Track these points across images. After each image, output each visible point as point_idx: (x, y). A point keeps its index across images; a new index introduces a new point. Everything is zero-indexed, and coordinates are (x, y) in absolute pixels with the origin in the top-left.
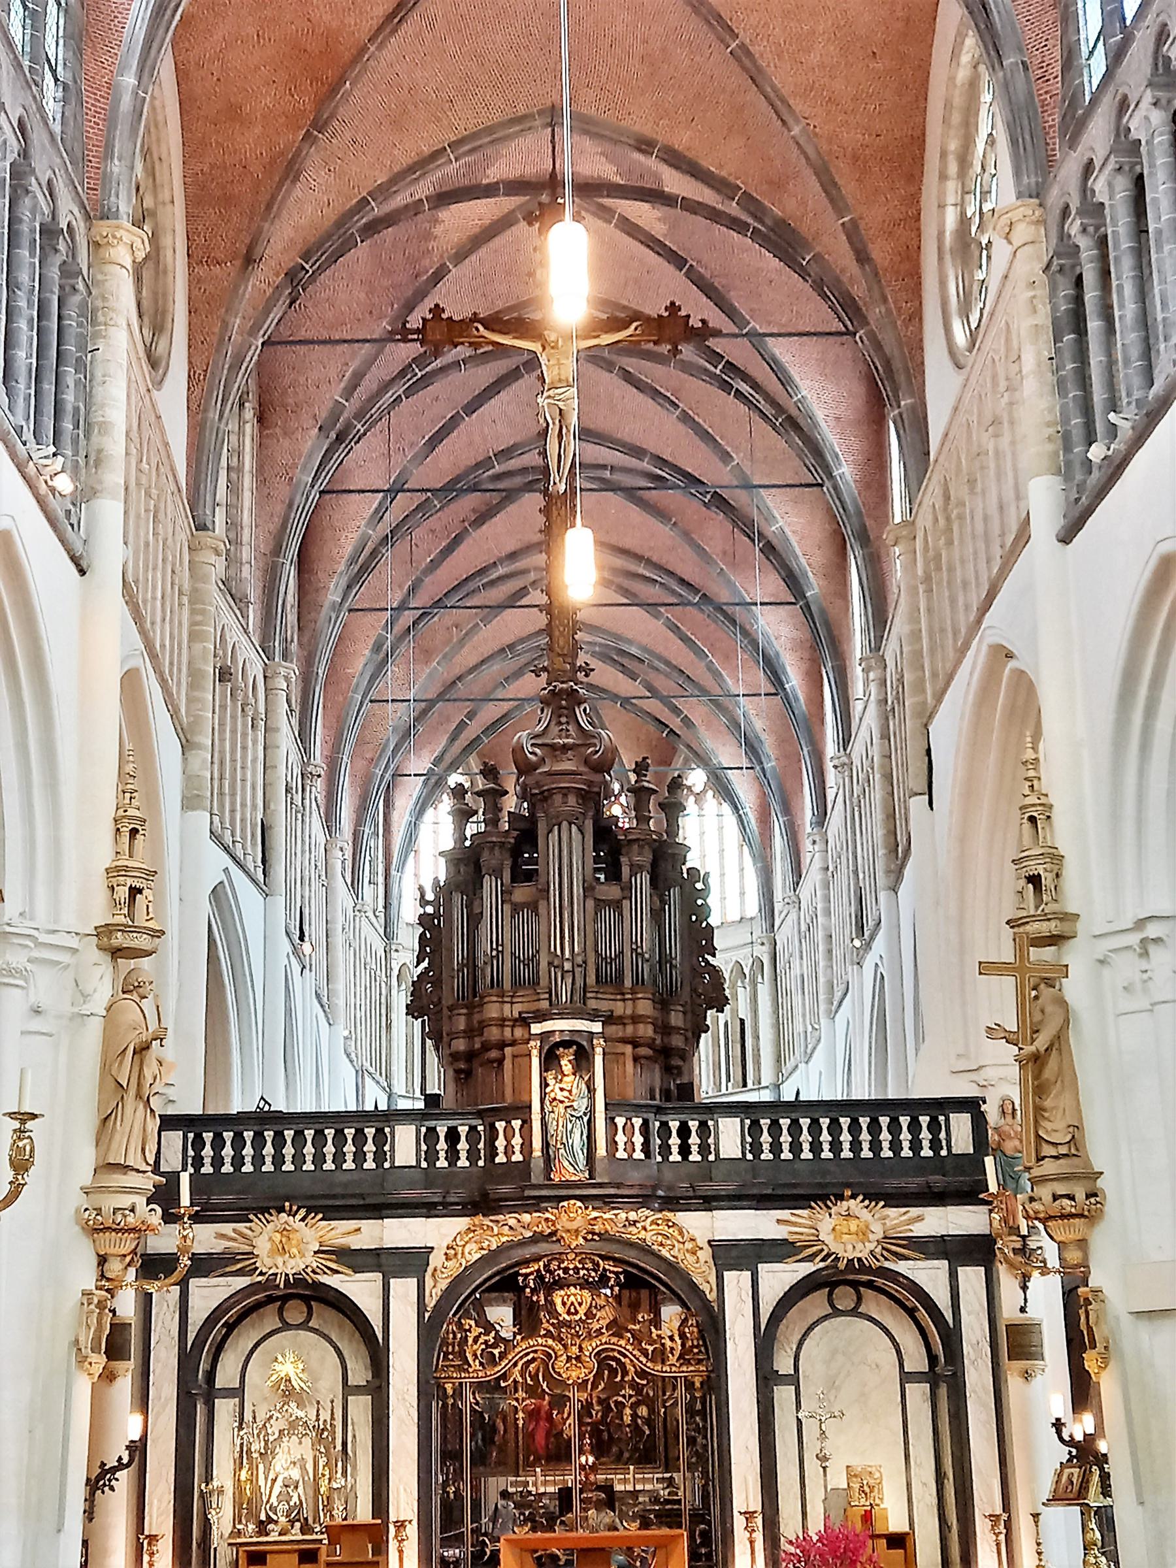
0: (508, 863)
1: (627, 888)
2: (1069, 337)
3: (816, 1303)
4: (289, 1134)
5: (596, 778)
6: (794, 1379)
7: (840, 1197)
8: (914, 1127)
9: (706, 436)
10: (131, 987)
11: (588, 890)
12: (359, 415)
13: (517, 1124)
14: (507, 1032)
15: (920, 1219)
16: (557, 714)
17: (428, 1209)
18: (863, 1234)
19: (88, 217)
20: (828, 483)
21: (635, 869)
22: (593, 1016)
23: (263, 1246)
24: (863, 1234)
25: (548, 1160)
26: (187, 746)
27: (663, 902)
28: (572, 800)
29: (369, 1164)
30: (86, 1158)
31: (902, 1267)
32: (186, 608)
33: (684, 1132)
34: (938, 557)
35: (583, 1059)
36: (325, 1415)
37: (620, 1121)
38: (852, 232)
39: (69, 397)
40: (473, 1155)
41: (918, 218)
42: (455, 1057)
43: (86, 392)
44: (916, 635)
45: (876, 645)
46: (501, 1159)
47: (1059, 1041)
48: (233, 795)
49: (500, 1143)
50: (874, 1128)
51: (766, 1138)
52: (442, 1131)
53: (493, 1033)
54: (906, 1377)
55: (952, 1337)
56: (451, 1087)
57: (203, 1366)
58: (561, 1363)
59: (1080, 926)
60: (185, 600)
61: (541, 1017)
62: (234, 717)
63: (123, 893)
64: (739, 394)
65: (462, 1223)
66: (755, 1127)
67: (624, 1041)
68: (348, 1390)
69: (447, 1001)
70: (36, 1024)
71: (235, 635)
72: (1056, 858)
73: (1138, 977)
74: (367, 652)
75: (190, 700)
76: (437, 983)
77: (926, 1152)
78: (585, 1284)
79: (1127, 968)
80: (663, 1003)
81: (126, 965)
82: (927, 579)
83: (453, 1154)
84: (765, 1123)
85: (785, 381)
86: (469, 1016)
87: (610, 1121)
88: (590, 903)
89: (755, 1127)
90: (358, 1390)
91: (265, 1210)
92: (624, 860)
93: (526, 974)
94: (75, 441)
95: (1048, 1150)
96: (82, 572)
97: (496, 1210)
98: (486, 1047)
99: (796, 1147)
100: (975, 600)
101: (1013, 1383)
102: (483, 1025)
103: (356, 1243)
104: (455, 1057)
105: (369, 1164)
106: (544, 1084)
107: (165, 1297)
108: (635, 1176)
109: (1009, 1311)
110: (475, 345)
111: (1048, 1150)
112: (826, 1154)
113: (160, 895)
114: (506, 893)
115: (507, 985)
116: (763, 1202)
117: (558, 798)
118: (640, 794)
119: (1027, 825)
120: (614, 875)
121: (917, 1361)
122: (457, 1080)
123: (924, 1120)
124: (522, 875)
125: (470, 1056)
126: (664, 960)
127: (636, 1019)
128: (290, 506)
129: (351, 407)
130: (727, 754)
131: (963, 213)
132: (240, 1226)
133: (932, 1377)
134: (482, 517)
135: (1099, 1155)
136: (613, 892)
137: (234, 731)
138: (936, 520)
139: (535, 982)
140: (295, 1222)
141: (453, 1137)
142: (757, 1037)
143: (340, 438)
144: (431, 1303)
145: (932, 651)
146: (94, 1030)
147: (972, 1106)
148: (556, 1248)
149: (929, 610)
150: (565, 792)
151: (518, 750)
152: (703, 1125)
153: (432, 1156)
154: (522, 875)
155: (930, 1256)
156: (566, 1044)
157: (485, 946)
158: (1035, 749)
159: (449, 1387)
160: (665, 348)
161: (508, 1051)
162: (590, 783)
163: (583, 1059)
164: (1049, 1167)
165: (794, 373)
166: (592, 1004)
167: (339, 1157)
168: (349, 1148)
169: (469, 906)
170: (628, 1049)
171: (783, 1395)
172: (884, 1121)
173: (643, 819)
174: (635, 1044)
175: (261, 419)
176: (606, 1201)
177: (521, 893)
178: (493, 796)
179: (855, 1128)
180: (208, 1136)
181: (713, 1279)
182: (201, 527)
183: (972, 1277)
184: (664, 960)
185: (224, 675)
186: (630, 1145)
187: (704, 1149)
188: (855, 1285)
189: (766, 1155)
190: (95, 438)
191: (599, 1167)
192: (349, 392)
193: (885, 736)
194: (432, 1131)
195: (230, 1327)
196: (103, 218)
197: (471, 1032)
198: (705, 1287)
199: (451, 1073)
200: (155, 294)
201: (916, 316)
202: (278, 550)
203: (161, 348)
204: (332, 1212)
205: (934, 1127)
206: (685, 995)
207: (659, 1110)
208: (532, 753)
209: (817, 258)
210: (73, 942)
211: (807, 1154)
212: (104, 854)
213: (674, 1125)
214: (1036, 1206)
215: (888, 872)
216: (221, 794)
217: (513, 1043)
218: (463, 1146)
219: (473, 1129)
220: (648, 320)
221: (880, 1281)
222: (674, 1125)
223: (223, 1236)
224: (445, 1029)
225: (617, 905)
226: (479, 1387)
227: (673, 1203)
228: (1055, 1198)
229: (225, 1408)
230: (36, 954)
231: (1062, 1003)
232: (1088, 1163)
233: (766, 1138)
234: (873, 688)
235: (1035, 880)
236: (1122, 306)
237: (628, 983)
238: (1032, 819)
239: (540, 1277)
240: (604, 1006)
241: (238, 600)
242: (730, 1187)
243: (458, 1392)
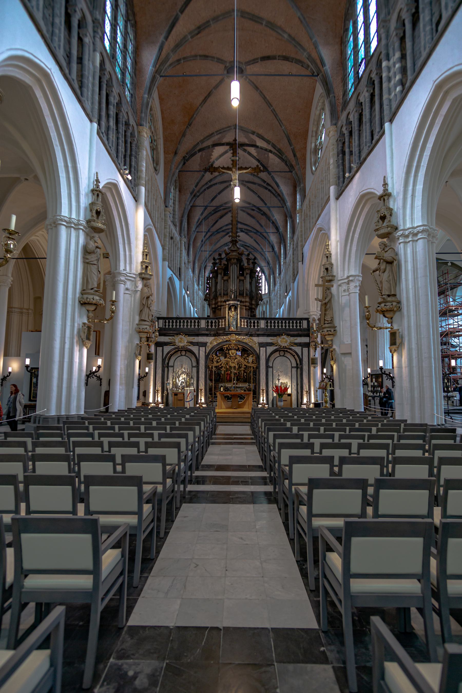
0: (223, 272)
1: (245, 278)
2: (341, 155)
3: (277, 354)
4: (182, 321)
5: (240, 256)
6: (272, 367)
7: (282, 335)
8: (296, 323)
9: (262, 200)
10: (145, 285)
11: (238, 277)
12: (198, 191)
13: (223, 320)
14: (222, 304)
15: (297, 339)
16: (233, 245)
17: (207, 335)
18: (286, 342)
19: (137, 125)
20: (285, 207)
21: (247, 274)
22: (238, 301)
23: (177, 341)
24: (286, 342)
25: (229, 327)
26: (163, 249)
27: (252, 281)
28: (235, 260)
29: (196, 327)
30: (137, 318)
31: (293, 348)
32: (163, 223)
33: (254, 323)
34: (307, 214)
35: (236, 309)
36: (189, 371)
37: (243, 320)
38: (293, 151)
39: (133, 164)
40: (215, 326)
41: (306, 148)
42: (212, 308)
43: (137, 163)
44: (301, 231)
45: (292, 238)
46: (220, 326)
47: (330, 300)
48: (173, 261)
49: (220, 324)
50: (289, 323)
51: (269, 324)
52: (210, 321)
53: (219, 304)
54: (292, 367)
55: (301, 360)
56: (212, 314)
57: (166, 362)
58: (230, 363)
59: (336, 278)
60: (163, 221)
61: (228, 301)
62: (174, 247)
63: (144, 266)
64: (269, 190)
65: (213, 338)
66: (267, 322)
67: (244, 306)
68: (192, 367)
69: (211, 298)
70: (127, 292)
71: (174, 231)
72: (332, 264)
73: (346, 288)
74: (200, 242)
75: (164, 240)
76: (209, 295)
77: (298, 327)
78: (235, 349)
79: (345, 287)
80: (251, 298)
81: (145, 281)
82: (304, 220)
83: (212, 326)
84: (269, 321)
85: (278, 186)
86: (215, 301)
87: (241, 320)
88: (238, 280)
89: (267, 322)
90: (194, 367)
91: (177, 334)
92: (245, 272)
93: (225, 293)
94: (135, 173)
95: (326, 322)
96: (136, 201)
97: (220, 336)
98: (218, 306)
99: (275, 326)
100: (314, 220)
101: (312, 368)
102: (218, 302)
103: (194, 341)
104: (212, 308)
105: (196, 327)
106: (229, 313)
107: (159, 349)
108: (245, 330)
109: (312, 356)
110: (219, 172)
111: (326, 322)
112: (280, 327)
113: (152, 267)
114: (222, 278)
115: (222, 295)
116: (268, 335)
117: (232, 260)
118: (248, 260)
119: (326, 258)
120: (242, 275)
121: (294, 364)
122: (213, 313)
123: (298, 322)
124: (225, 275)
125: (215, 308)
126: (251, 291)
127: (246, 302)
128: (185, 208)
129: (197, 189)
130: (263, 264)
131: (316, 144)
132: (173, 337)
133: (297, 368)
134: (221, 217)
135: (336, 323)
136: (242, 278)
137: (174, 249)
138: (307, 207)
139: (227, 294)
140: (183, 337)
141: (212, 322)
142: (266, 313)
143: (194, 196)
144: (207, 352)
145: (305, 234)
146: (138, 294)
147: (307, 319)
148: (230, 343)
149: (304, 226)
150: (234, 259)
151: (225, 251)
152: (258, 322)
153: (208, 326)
154: (225, 275)
155: (298, 346)
156: (233, 306)
157: (219, 287)
158: (328, 242)
159: (210, 367)
160: (256, 174)
161: (222, 307)
162: (239, 257)
163: (236, 309)
164: (326, 325)
165: (280, 184)
166: (238, 299)
167: (191, 326)
168: (193, 324)
169: (216, 281)
170: (244, 307)
171: (270, 370)
172: (291, 322)
173: (248, 264)
174: (246, 306)
175: (180, 191)
176: (239, 335)
177: (225, 278)
178: (221, 259)
179: (285, 323)
180: (167, 321)
181: (258, 349)
182: (166, 207)
183: (305, 350)
184: (251, 291)
185: (172, 238)
186: (244, 325)
187: (258, 326)
188: (284, 351)
189: (269, 327)
190: (139, 173)
191: (238, 328)
192: (196, 186)
193: (293, 254)
194: (208, 322)
195: (171, 355)
196: (141, 125)
197: (216, 304)
198: (257, 350)
199: (212, 311)
200: (157, 158)
201: (305, 168)
202: (182, 217)
203: (157, 168)
204: (189, 335)
205: (300, 323)
206: (255, 298)
207: (250, 319)
208: (228, 251)
209: (286, 156)
210: (134, 276)
211: (276, 327)
212: (140, 259)
213: (252, 321)
214: (323, 333)
215: (293, 280)
216: (171, 260)
217: (223, 306)
218: (214, 324)
219: (215, 321)
220: (252, 168)
221: (288, 350)
222: (252, 321)
223: (170, 339)
224: (211, 303)
225: (243, 281)
226: (216, 367)
227: (251, 335)
228: (327, 331)
229: (171, 369)
230: (127, 278)
231: (331, 293)
232: (334, 325)
233: (269, 324)
234: (292, 246)
235: (327, 269)
236: (355, 142)
237: (245, 295)
238: (327, 257)
239: (227, 348)
240: (240, 299)
241: (175, 225)
242: (262, 333)
243: (212, 368)
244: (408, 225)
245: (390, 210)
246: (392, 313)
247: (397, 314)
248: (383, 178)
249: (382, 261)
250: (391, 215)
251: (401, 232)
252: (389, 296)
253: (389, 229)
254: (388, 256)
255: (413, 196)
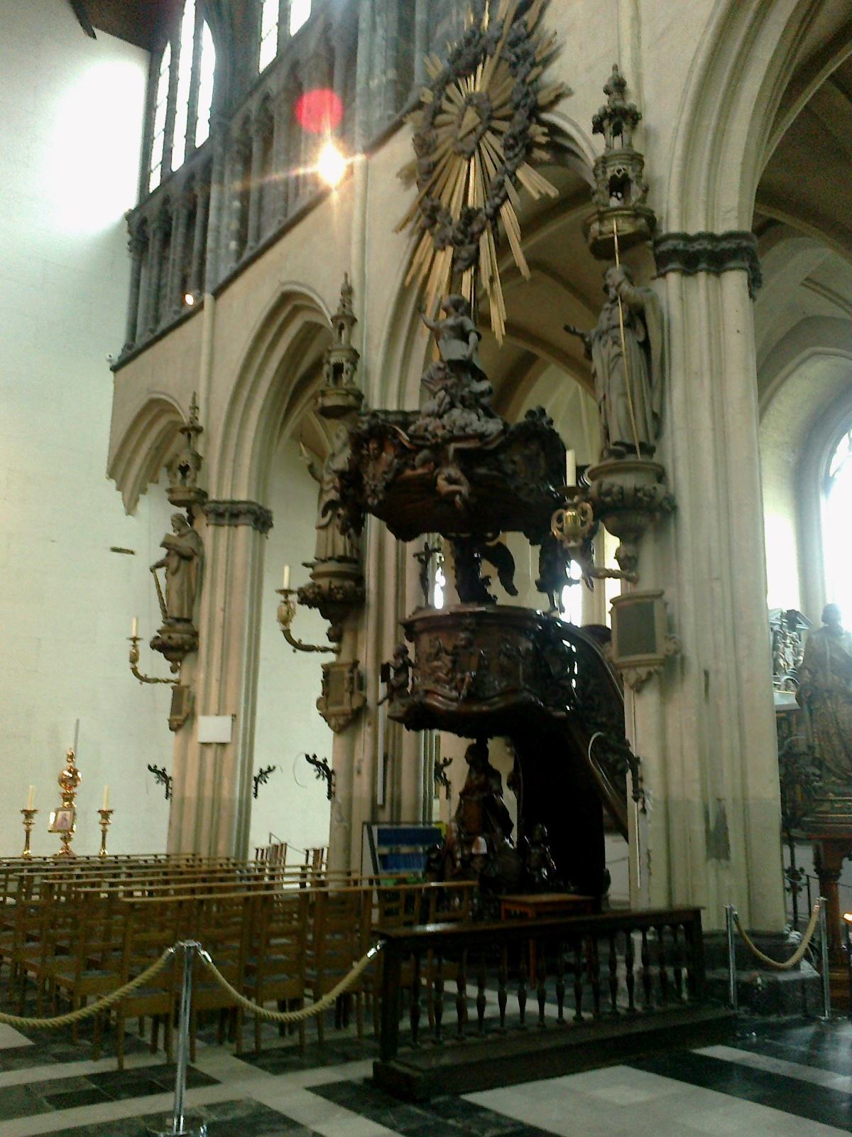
244: (226, 496)
245: (198, 459)
246: (180, 654)
247: (190, 657)
248: (191, 395)
249: (172, 552)
250: (198, 468)
251: (212, 505)
252: (178, 620)
253: (192, 494)
254: (186, 544)
255: (239, 445)
